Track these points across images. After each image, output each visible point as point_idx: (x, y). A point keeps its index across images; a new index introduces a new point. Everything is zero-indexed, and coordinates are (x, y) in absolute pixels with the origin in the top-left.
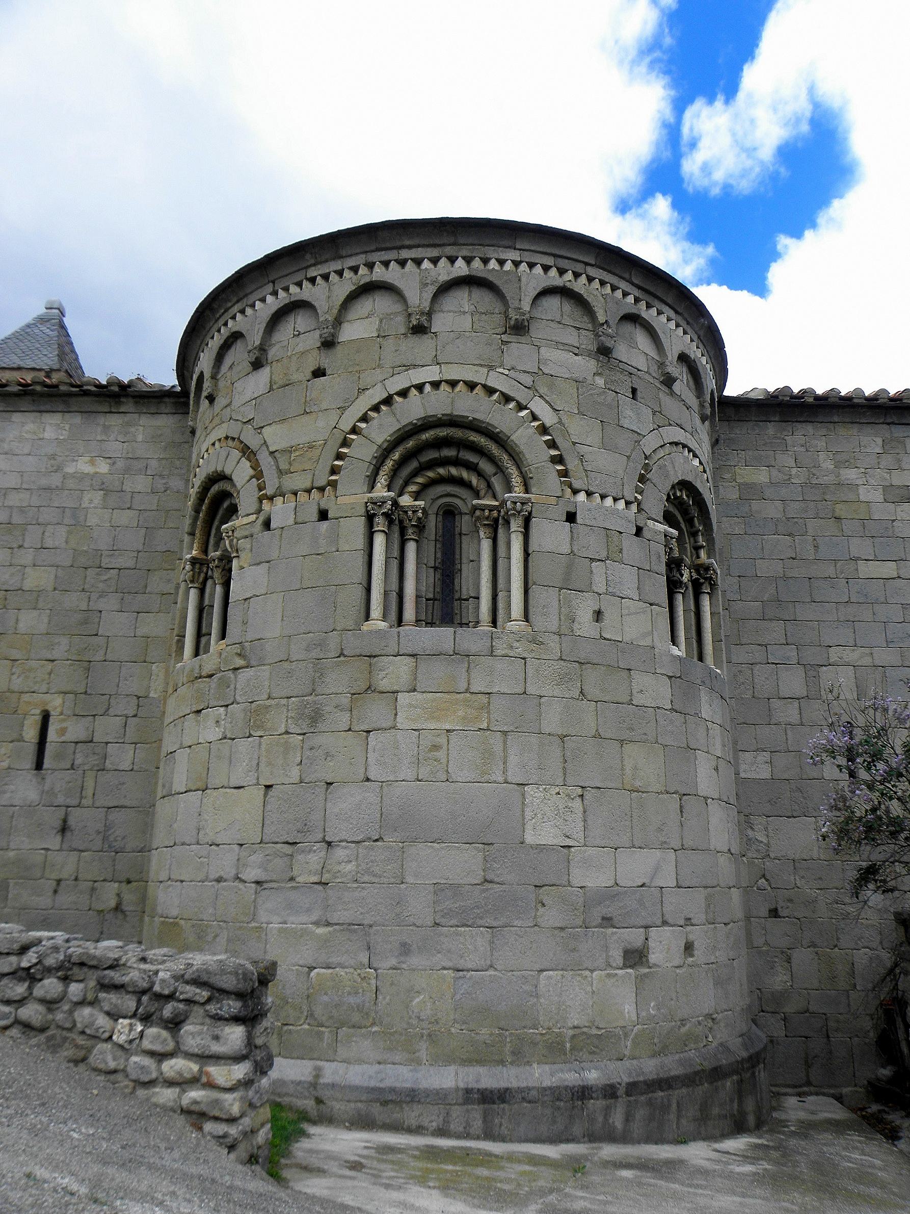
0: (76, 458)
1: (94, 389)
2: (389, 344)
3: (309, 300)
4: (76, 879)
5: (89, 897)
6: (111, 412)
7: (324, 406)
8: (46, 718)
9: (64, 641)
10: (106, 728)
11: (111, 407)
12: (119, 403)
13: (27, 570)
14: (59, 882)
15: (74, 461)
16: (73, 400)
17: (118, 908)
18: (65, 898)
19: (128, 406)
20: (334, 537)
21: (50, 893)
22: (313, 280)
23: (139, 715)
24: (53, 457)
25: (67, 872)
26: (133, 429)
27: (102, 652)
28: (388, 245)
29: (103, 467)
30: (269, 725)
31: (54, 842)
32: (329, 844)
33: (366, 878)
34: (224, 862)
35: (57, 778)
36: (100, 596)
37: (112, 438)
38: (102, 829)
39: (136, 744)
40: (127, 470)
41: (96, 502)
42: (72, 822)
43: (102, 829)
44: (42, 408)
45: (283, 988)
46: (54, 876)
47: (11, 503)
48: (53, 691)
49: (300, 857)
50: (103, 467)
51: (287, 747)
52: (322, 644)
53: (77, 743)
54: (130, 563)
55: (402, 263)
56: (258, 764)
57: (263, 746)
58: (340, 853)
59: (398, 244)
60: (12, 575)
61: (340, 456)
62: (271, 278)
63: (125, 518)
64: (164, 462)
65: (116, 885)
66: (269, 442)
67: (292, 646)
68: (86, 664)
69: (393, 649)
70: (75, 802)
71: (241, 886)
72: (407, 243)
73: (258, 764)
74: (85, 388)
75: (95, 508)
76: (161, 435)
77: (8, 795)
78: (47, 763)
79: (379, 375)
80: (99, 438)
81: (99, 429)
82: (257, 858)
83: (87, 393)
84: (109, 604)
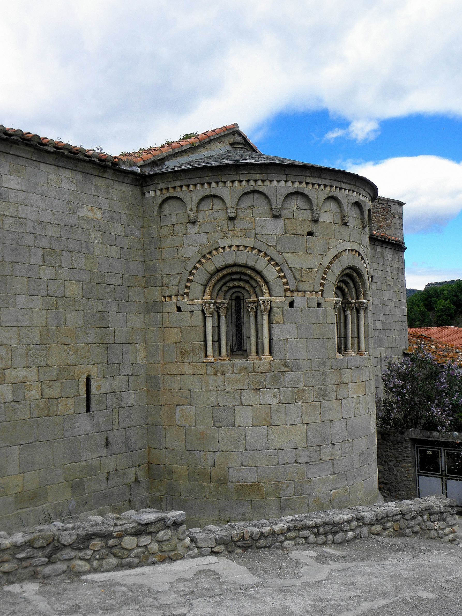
0: (83, 206)
1: (98, 161)
3: (308, 195)
4: (116, 470)
5: (123, 478)
6: (99, 176)
7: (316, 252)
8: (88, 379)
9: (93, 331)
10: (120, 383)
11: (99, 172)
12: (105, 172)
13: (67, 283)
14: (108, 473)
15: (82, 207)
16: (80, 164)
17: (137, 481)
18: (113, 481)
19: (109, 174)
20: (325, 317)
21: (105, 481)
22: (307, 184)
23: (134, 374)
24: (69, 203)
25: (112, 468)
26: (111, 191)
27: (113, 338)
28: (339, 179)
29: (99, 216)
30: (305, 398)
31: (103, 452)
33: (344, 455)
34: (289, 457)
35: (100, 416)
36: (108, 303)
37: (100, 194)
38: (124, 441)
39: (134, 391)
40: (111, 219)
41: (98, 239)
42: (110, 439)
43: (124, 441)
44: (60, 164)
45: (322, 500)
46: (106, 471)
47: (50, 234)
48: (91, 363)
49: (323, 451)
50: (99, 216)
51: (315, 408)
52: (324, 364)
53: (107, 393)
54: (119, 282)
55: (341, 189)
56: (302, 415)
57: (304, 407)
58: (337, 447)
59: (342, 180)
60: (58, 286)
61: (323, 278)
62: (286, 173)
63: (114, 251)
64: (129, 216)
65: (134, 469)
66: (288, 261)
67: (313, 364)
68: (105, 346)
69: (346, 367)
70: (110, 428)
71: (299, 465)
72: (344, 181)
73: (302, 415)
74: (93, 159)
75: (98, 243)
76: (125, 198)
77: (76, 430)
78: (93, 407)
79: (334, 242)
80: (94, 194)
81: (93, 187)
82: (306, 453)
83: (91, 162)
84: (112, 307)
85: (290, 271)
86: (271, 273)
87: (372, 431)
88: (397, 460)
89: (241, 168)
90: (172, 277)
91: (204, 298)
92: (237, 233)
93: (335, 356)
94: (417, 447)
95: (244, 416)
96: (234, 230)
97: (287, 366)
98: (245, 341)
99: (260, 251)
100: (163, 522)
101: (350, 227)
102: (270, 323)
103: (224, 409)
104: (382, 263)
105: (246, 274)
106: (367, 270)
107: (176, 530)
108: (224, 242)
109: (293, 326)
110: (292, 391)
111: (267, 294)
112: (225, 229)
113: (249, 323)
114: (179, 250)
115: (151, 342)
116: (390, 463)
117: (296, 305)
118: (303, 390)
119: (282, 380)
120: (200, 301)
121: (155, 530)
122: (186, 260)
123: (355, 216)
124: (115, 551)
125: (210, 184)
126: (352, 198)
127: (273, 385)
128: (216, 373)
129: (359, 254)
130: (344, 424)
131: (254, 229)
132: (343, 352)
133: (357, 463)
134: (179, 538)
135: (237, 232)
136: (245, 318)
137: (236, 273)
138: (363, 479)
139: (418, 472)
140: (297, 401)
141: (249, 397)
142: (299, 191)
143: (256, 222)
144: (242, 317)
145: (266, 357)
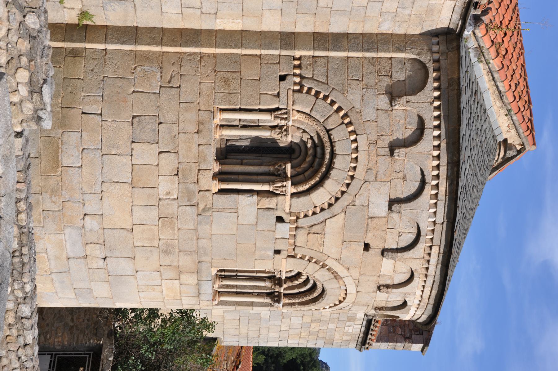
2: (375, 278)
20: (263, 258)
23: (202, 15)
30: (164, 230)
32: (105, 259)
39: (182, 13)
85: (321, 221)
86: (321, 197)
87: (116, 304)
88: (72, 327)
89: (455, 169)
90: (324, 70)
91: (294, 111)
92: (373, 158)
93: (214, 267)
94: (89, 354)
95: (145, 155)
96: (377, 156)
97: (204, 210)
98: (238, 157)
99: (348, 185)
100: (42, 107)
101: (375, 294)
102: (259, 192)
103: (154, 130)
104: (341, 319)
105: (321, 165)
106: (322, 309)
107: (33, 119)
108: (362, 142)
109: (252, 220)
110: (173, 214)
111: (294, 190)
112: (380, 144)
113: (261, 165)
114: (358, 82)
115: (244, 39)
116: (70, 318)
117: (280, 225)
118: (174, 228)
119: (188, 203)
120: (290, 108)
121: (34, 100)
122: (344, 92)
123: (389, 300)
124: (15, 61)
125: (438, 127)
126: (411, 299)
127: (182, 192)
128: (200, 123)
129: (341, 302)
130: (129, 273)
131: (376, 180)
132: (219, 273)
133: (79, 285)
134: (23, 121)
135: (375, 159)
136: (266, 159)
137: (323, 154)
138: (58, 291)
139: (56, 355)
140: (161, 219)
141: (169, 163)
142: (422, 238)
143: (385, 183)
144: (268, 155)
145: (216, 186)
